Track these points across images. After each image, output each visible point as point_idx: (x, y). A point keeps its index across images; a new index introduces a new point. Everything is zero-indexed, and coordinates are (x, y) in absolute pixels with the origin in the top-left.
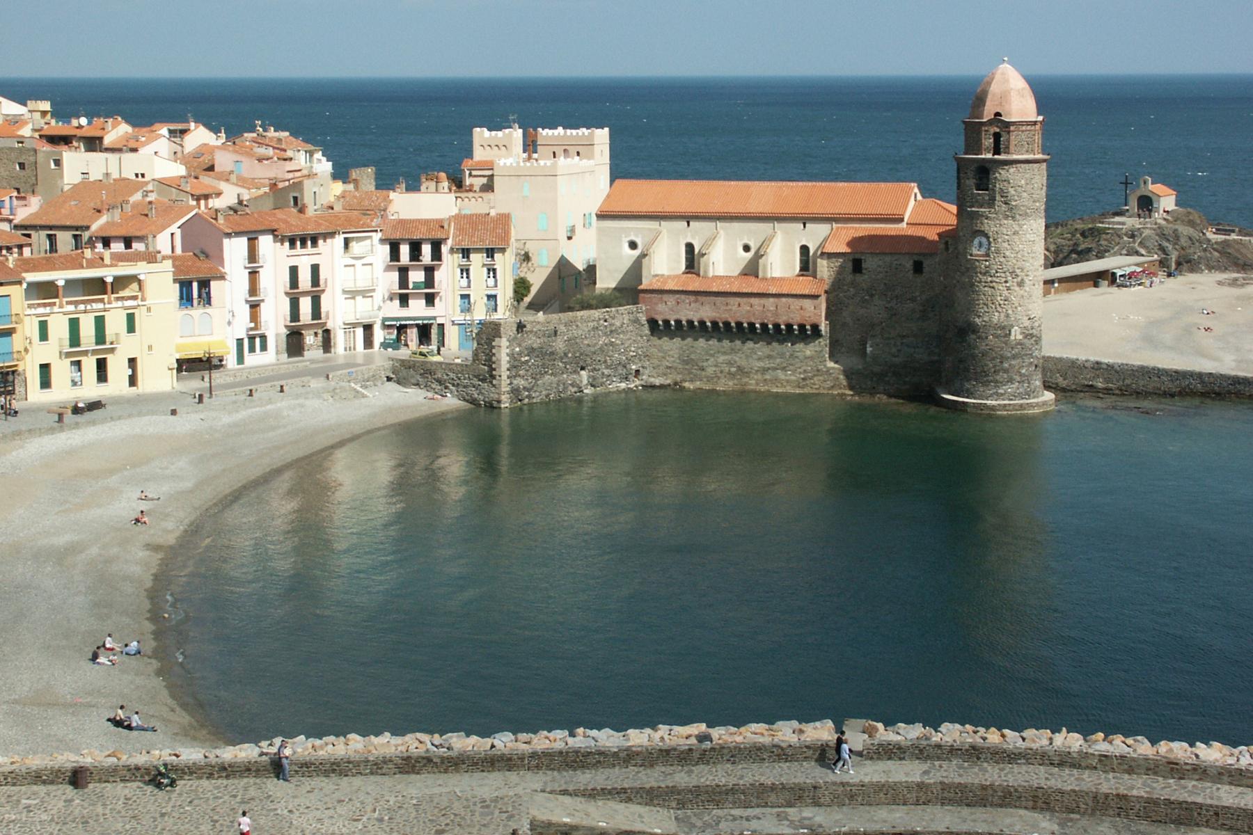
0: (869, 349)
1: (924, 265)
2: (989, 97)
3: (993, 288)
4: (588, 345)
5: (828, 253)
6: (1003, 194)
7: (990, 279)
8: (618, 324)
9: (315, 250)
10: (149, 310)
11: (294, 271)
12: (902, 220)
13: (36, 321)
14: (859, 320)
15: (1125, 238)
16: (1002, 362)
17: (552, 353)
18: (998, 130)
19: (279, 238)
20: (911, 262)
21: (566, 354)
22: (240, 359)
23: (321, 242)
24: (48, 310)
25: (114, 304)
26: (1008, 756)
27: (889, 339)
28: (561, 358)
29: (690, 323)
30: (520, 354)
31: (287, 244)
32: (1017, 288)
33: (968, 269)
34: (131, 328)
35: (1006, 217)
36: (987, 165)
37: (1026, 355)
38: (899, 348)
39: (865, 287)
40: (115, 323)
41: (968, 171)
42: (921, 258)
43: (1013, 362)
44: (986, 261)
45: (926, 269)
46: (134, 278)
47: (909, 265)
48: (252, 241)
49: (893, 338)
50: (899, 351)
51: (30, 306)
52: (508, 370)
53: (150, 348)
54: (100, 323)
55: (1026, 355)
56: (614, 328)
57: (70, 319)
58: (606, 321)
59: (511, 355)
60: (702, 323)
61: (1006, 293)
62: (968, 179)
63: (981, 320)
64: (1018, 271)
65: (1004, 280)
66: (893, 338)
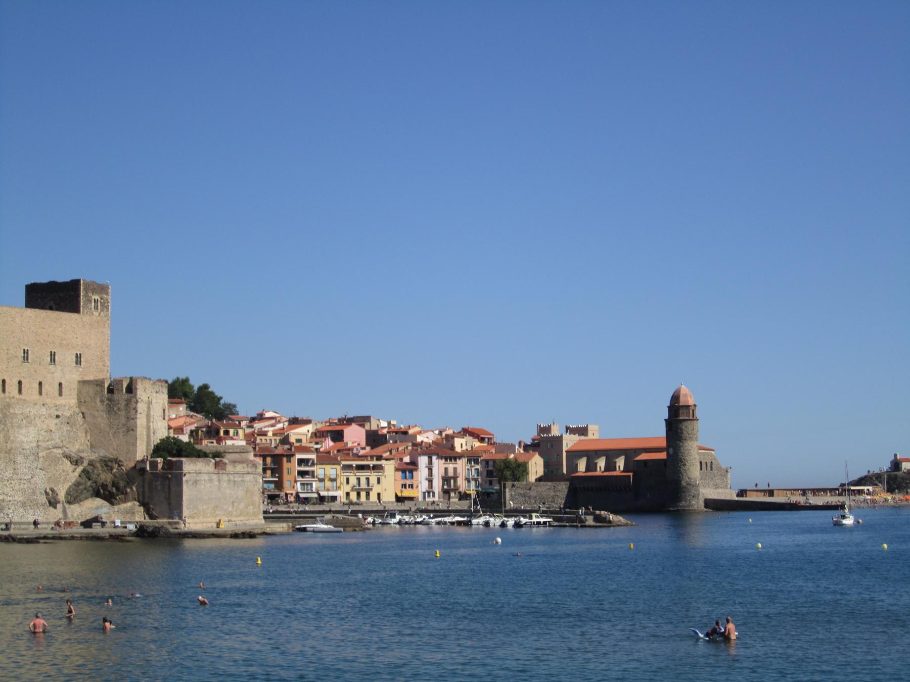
0: (648, 496)
10: (385, 477)
11: (446, 469)
19: (440, 457)
21: (536, 497)
22: (424, 498)
23: (458, 460)
25: (373, 474)
28: (534, 499)
30: (515, 495)
31: (444, 460)
34: (379, 481)
40: (373, 480)
48: (430, 459)
51: (343, 473)
53: (385, 490)
54: (368, 479)
59: (511, 495)
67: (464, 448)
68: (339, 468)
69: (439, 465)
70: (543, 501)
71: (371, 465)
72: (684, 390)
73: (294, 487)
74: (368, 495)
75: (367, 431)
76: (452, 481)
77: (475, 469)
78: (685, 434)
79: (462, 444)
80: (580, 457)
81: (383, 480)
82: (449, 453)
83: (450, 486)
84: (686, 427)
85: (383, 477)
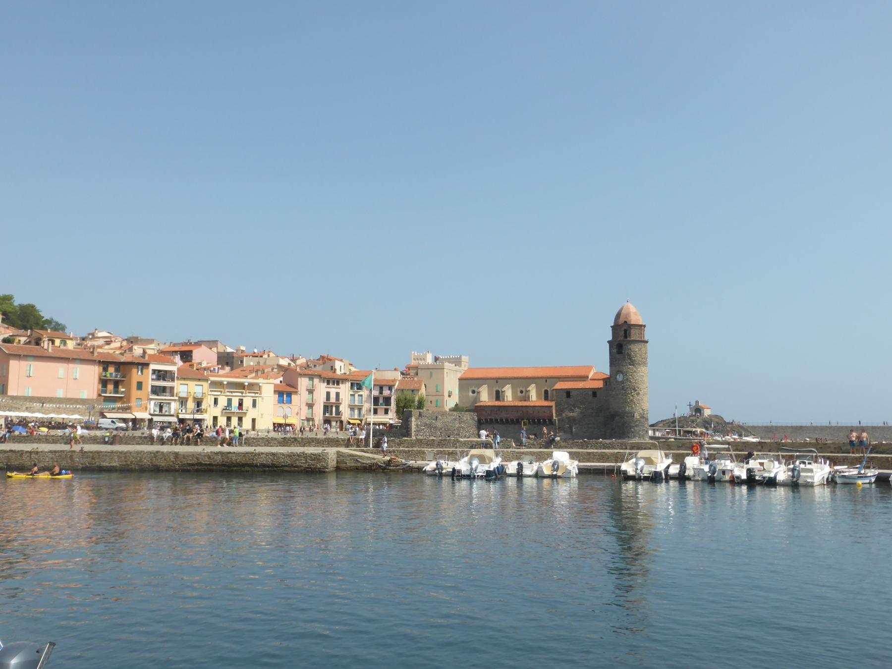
0: (574, 430)
1: (597, 394)
2: (622, 315)
3: (626, 395)
4: (451, 426)
5: (556, 389)
6: (629, 355)
8: (465, 419)
9: (338, 387)
11: (328, 394)
12: (588, 377)
13: (213, 398)
15: (690, 423)
16: (630, 428)
17: (435, 427)
18: (625, 328)
21: (441, 429)
23: (341, 382)
24: (219, 393)
25: (248, 395)
26: (603, 445)
29: (496, 420)
30: (421, 425)
31: (326, 381)
32: (636, 396)
33: (615, 388)
34: (254, 405)
35: (630, 365)
37: (641, 426)
40: (248, 402)
42: (596, 390)
43: (636, 428)
46: (257, 384)
47: (591, 393)
51: (211, 391)
52: (415, 431)
53: (262, 415)
55: (641, 426)
56: (463, 420)
57: (228, 399)
58: (459, 417)
59: (417, 425)
60: (501, 420)
61: (631, 398)
64: (637, 389)
65: (630, 392)
67: (343, 372)
68: (206, 385)
69: (322, 389)
70: (448, 434)
71: (246, 384)
72: (632, 309)
73: (146, 408)
74: (240, 419)
75: (218, 353)
76: (334, 409)
77: (359, 395)
78: (637, 358)
79: (341, 367)
80: (480, 386)
81: (259, 401)
82: (330, 375)
83: (331, 414)
84: (640, 350)
85: (260, 399)
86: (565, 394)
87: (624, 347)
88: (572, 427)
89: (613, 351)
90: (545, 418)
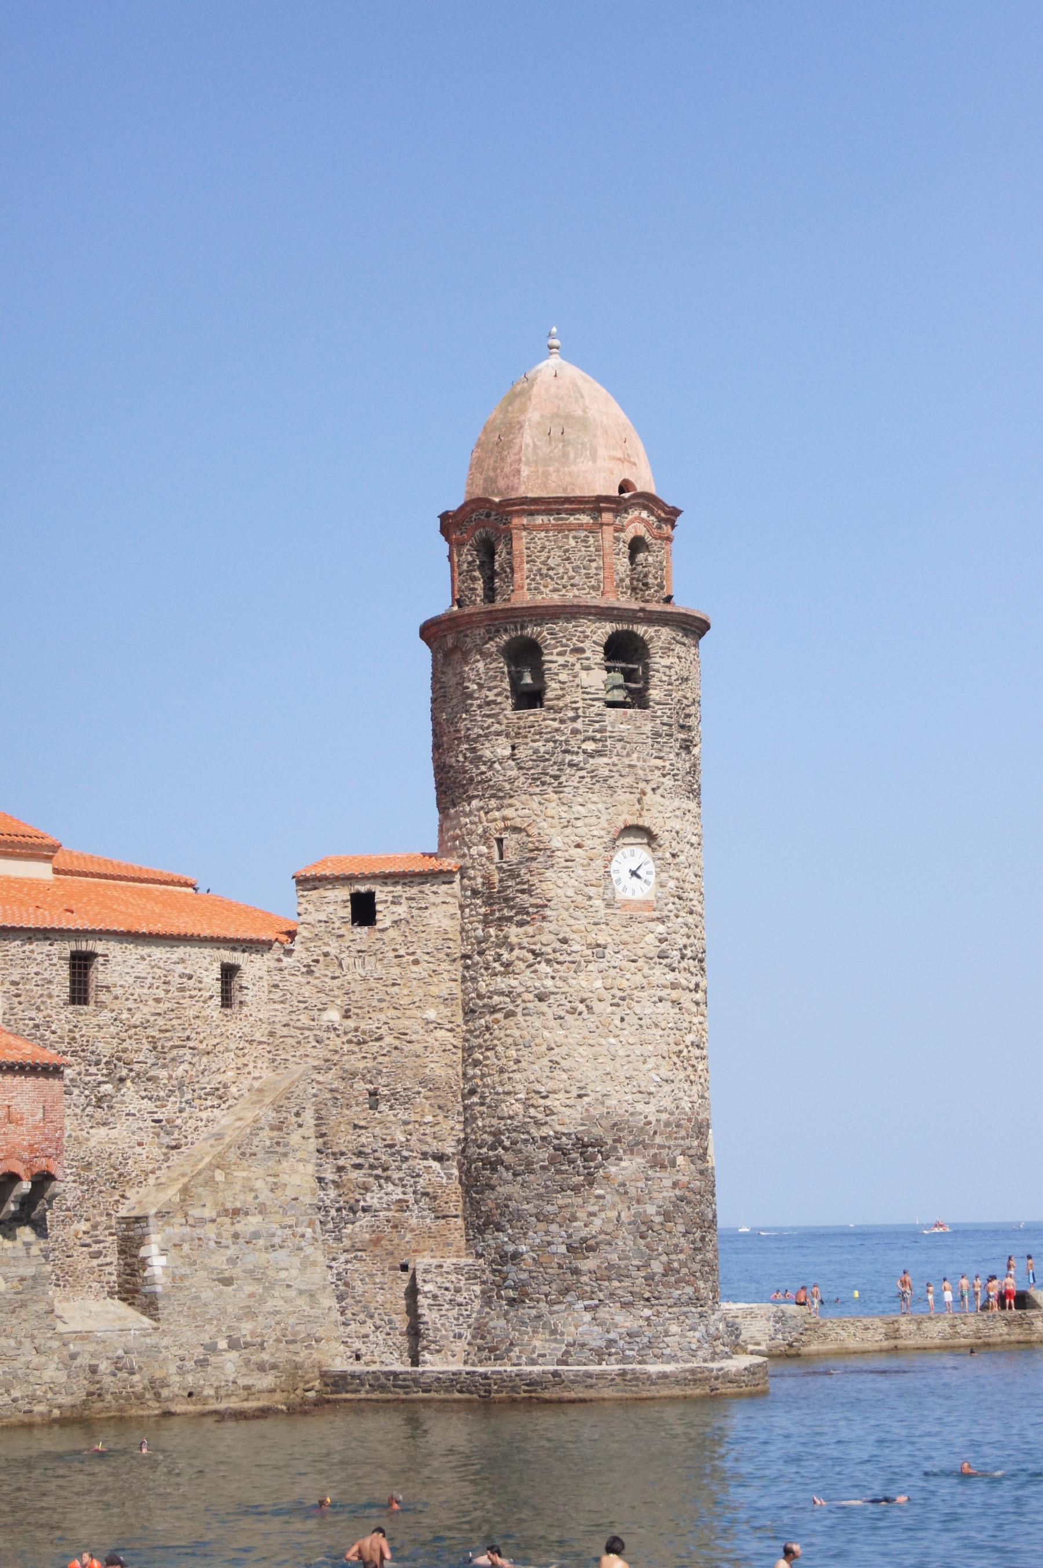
3: (675, 1003)
7: (671, 976)
14: (88, 1166)
18: (642, 530)
20: (217, 965)
27: (201, 1221)
36: (640, 630)
38: (229, 1253)
39: (105, 1050)
41: (587, 645)
44: (661, 920)
45: (248, 996)
49: (213, 1221)
50: (232, 1261)
62: (587, 668)
63: (651, 1109)
66: (213, 1221)
86: (63, 973)
87: (659, 661)
88: (141, 1241)
89: (585, 678)
90: (19, 1169)
